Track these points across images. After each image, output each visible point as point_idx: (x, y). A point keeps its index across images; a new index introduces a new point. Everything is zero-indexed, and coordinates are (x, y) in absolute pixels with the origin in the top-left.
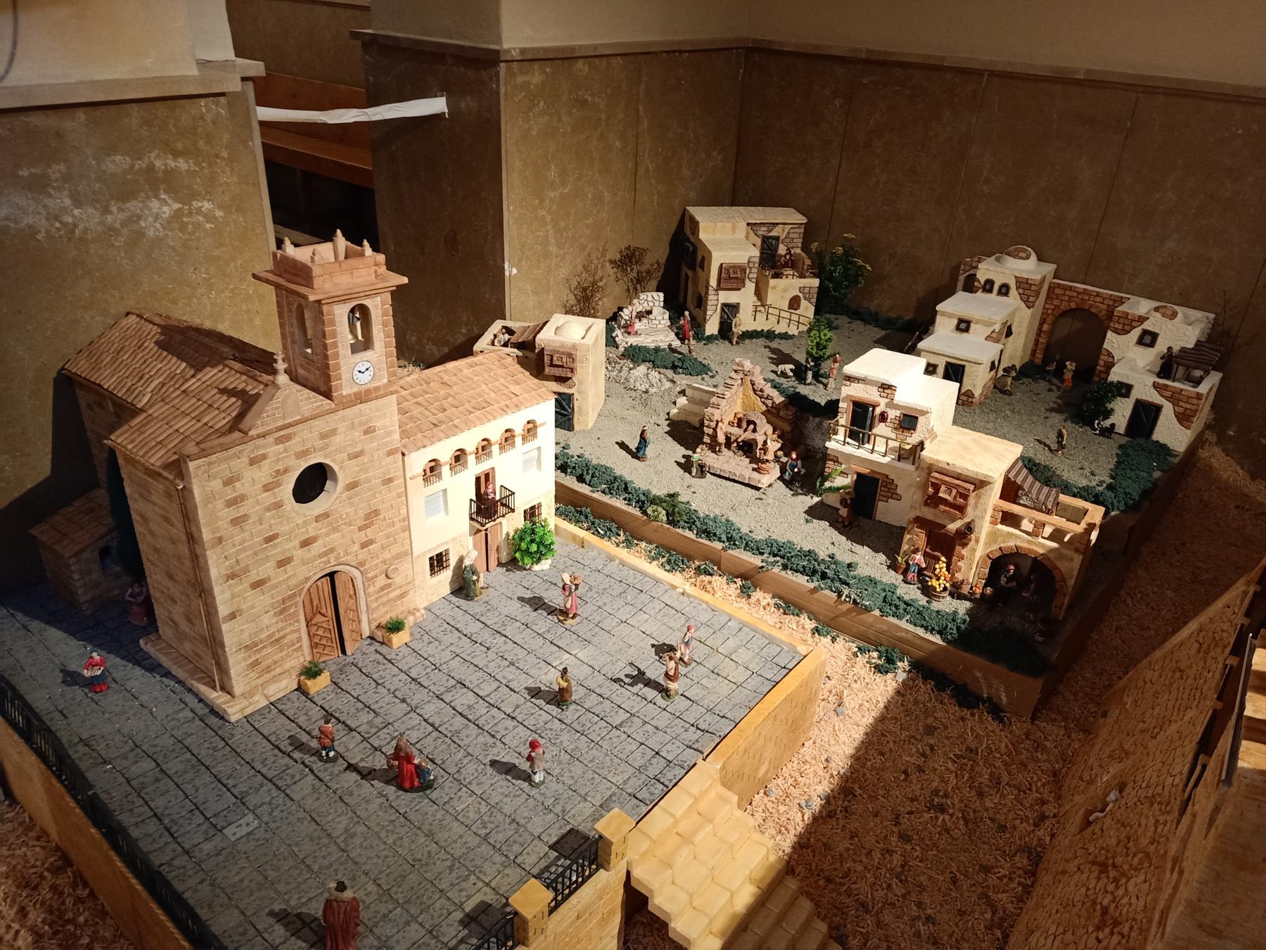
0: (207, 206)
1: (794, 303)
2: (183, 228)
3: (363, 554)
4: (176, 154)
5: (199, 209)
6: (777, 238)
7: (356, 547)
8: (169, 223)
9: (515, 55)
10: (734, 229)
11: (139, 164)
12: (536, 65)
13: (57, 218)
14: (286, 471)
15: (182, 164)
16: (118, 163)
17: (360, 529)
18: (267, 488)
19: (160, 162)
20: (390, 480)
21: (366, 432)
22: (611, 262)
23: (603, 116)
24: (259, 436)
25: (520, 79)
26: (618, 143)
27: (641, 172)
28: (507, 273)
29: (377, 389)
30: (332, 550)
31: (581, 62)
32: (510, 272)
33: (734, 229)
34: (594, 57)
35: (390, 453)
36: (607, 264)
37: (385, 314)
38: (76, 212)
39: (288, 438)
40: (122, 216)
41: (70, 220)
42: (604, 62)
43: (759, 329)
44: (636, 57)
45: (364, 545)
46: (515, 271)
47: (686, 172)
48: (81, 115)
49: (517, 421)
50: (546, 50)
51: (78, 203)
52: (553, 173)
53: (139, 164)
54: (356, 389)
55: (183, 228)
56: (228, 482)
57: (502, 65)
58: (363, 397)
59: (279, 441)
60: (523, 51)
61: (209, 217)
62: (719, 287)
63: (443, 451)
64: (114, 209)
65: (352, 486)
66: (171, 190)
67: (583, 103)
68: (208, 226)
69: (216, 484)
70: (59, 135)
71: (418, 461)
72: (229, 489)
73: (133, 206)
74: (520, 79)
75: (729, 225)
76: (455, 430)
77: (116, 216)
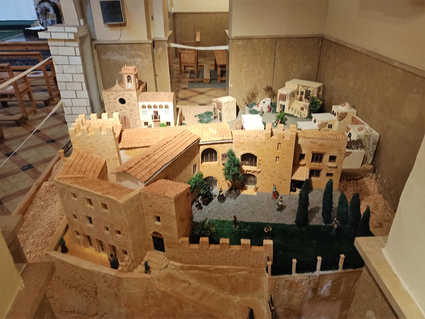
0: (146, 61)
1: (302, 109)
2: (142, 64)
3: (130, 116)
4: (142, 52)
5: (145, 61)
6: (310, 91)
7: (129, 114)
8: (140, 62)
9: (233, 38)
10: (294, 86)
11: (136, 53)
12: (241, 40)
13: (124, 59)
14: (117, 98)
15: (143, 54)
16: (133, 52)
17: (130, 111)
18: (114, 99)
19: (139, 53)
20: (135, 105)
21: (131, 96)
22: (264, 89)
23: (262, 53)
24: (112, 91)
25: (235, 43)
26: (267, 60)
27: (276, 67)
28: (230, 86)
29: (132, 89)
30: (124, 113)
31: (255, 40)
32: (230, 86)
33: (294, 86)
34: (259, 39)
35: (135, 101)
36: (263, 90)
37: (133, 78)
38: (126, 59)
39: (117, 93)
40: (133, 60)
41: (125, 60)
42: (263, 40)
43: (290, 114)
44: (276, 40)
45: (131, 114)
46: (232, 86)
47: (294, 69)
48: (128, 45)
49: (164, 104)
50: (242, 37)
51: (127, 57)
52: (245, 65)
53: (136, 53)
54: (128, 88)
55: (142, 64)
56: (108, 96)
57: (231, 41)
58: (130, 90)
59: (116, 93)
60: (235, 37)
61: (146, 62)
62: (279, 100)
63: (146, 104)
64: (132, 59)
65: (128, 104)
66: (141, 58)
67: (255, 49)
68: (146, 64)
69: (106, 96)
70: (125, 48)
71: (141, 104)
72: (108, 97)
73: (135, 59)
74: (235, 43)
75: (293, 85)
76: (149, 101)
77: (132, 60)
